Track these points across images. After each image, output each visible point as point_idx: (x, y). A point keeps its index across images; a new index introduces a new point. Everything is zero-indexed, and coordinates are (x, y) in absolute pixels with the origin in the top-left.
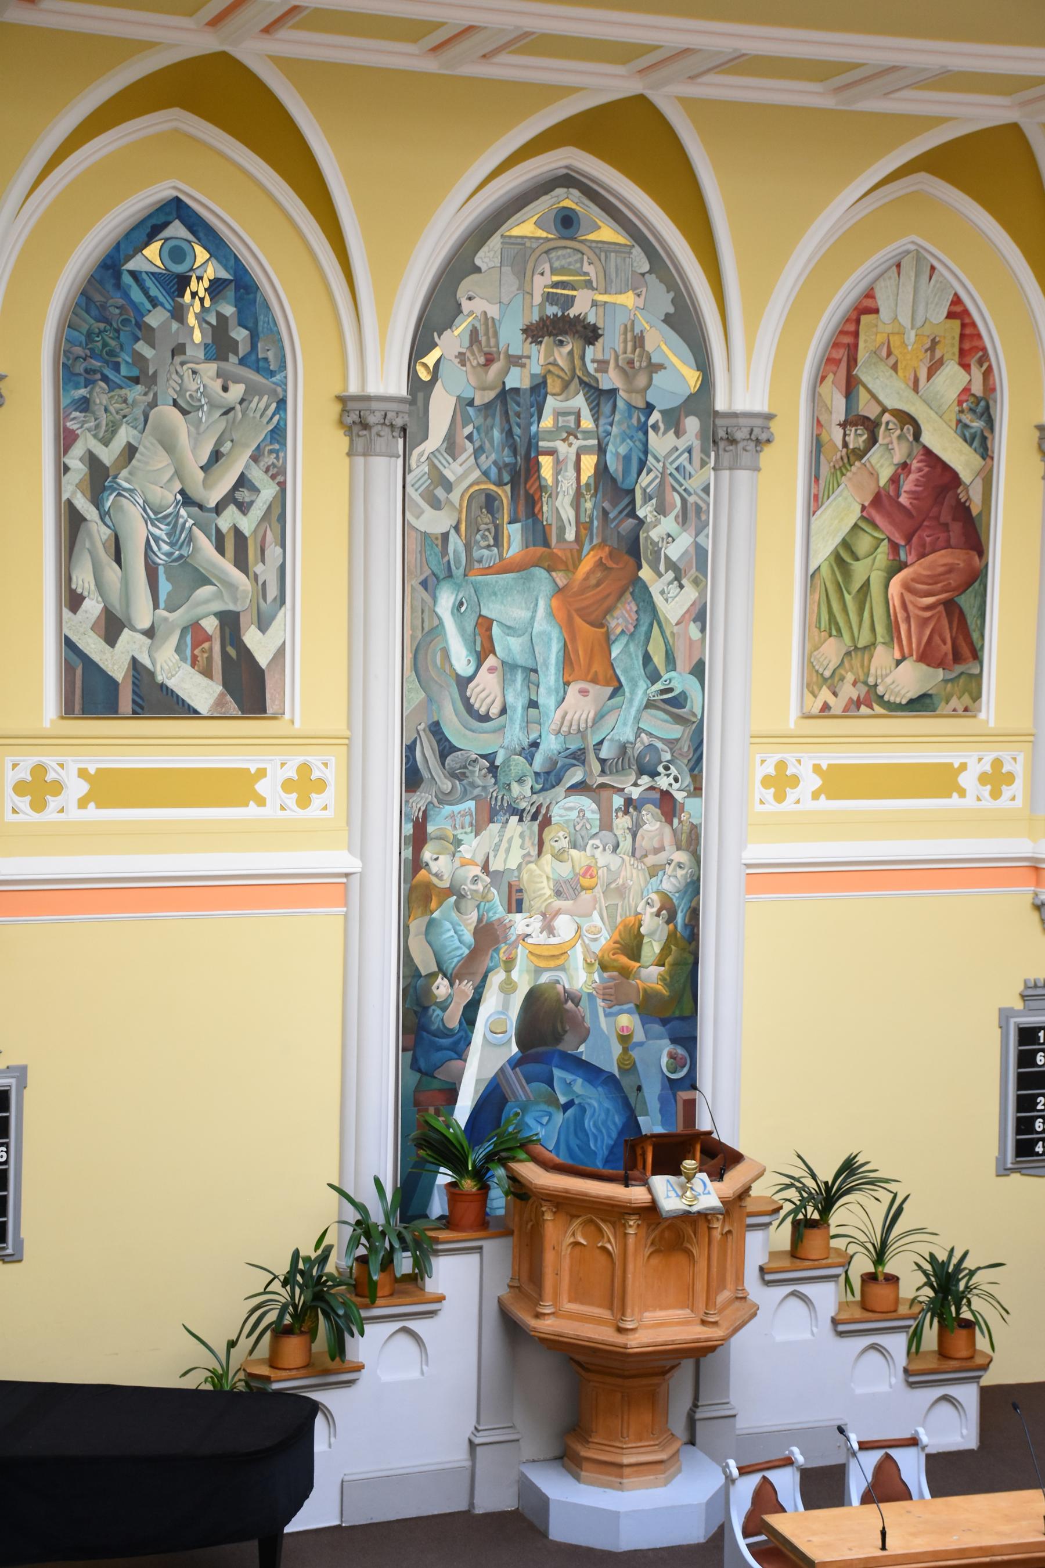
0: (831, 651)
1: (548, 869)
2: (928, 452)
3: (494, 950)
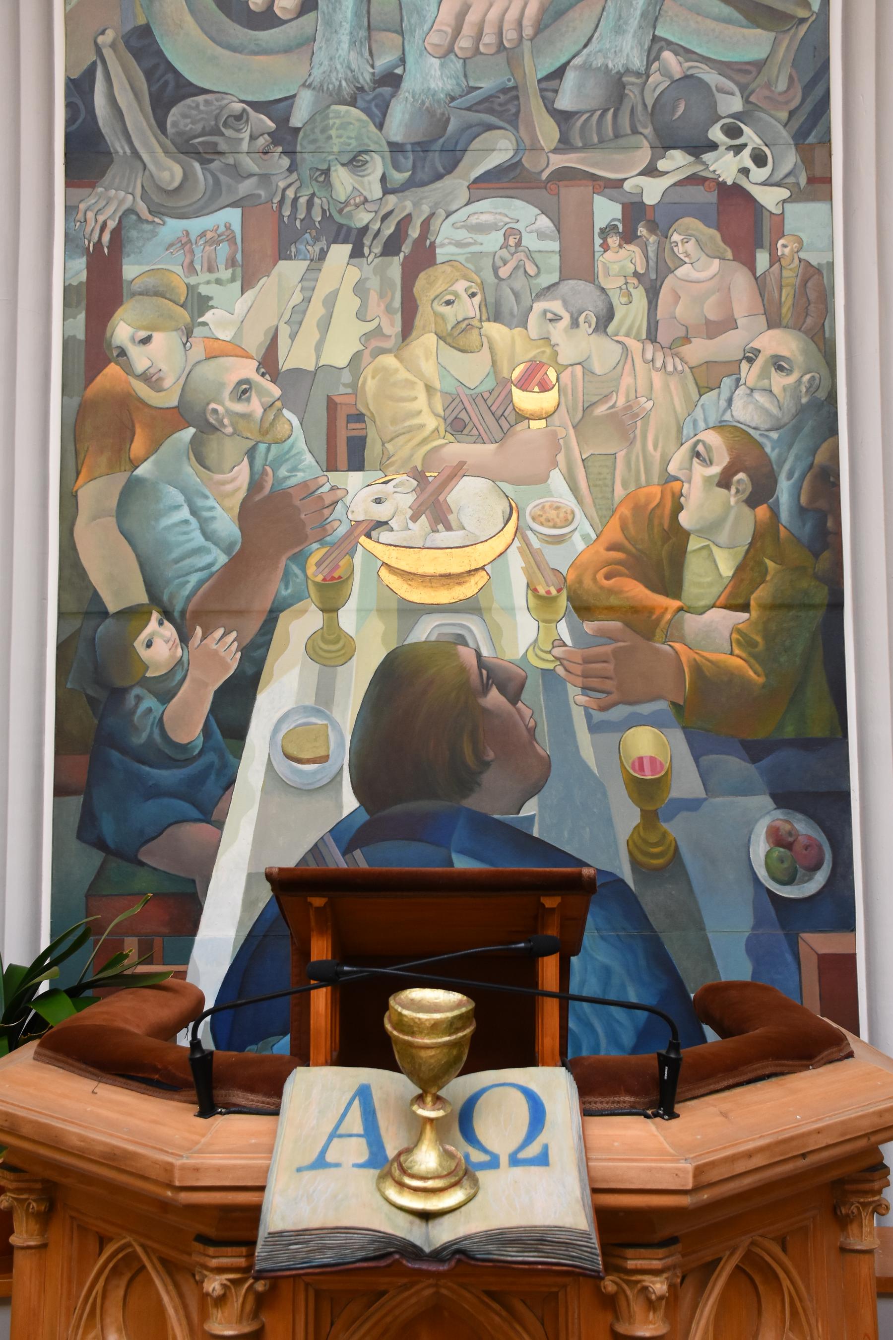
1: (429, 368)
3: (294, 558)
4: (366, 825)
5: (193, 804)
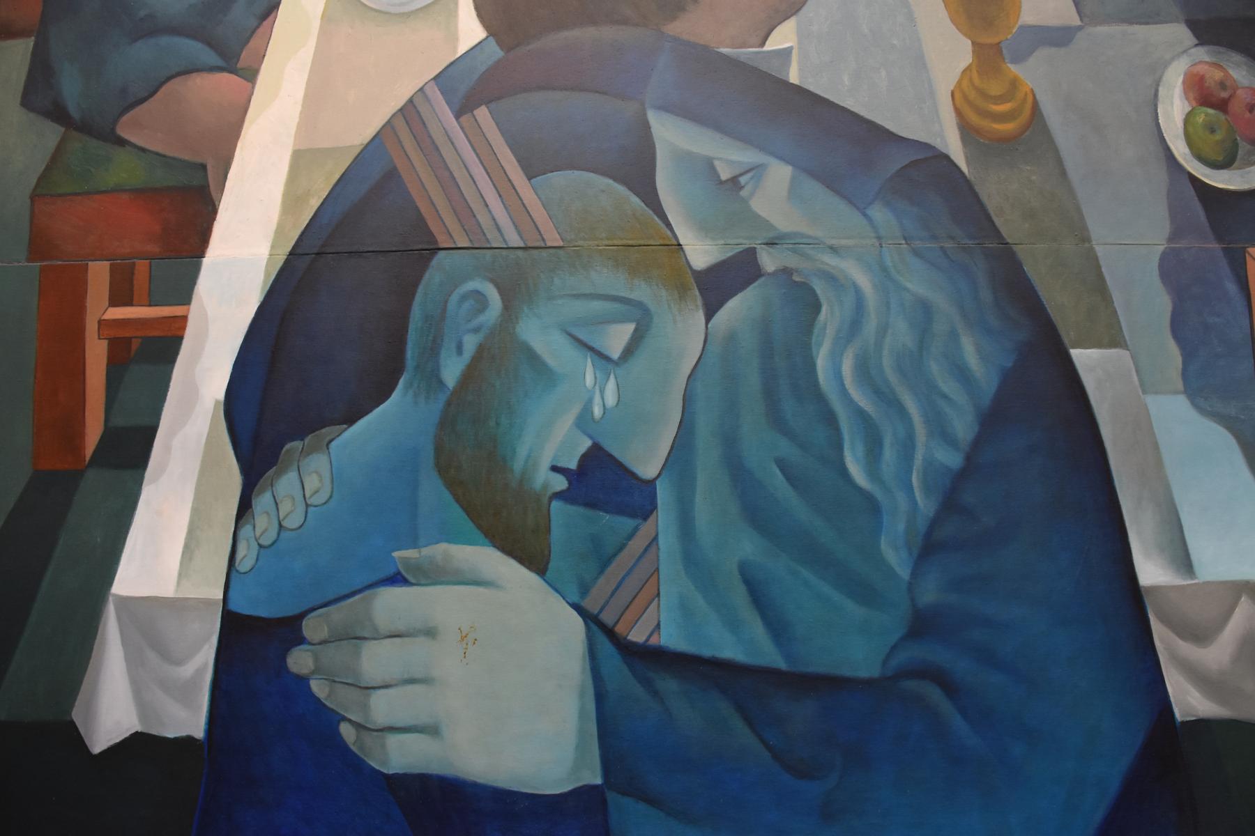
4: (497, 65)
5: (209, 45)
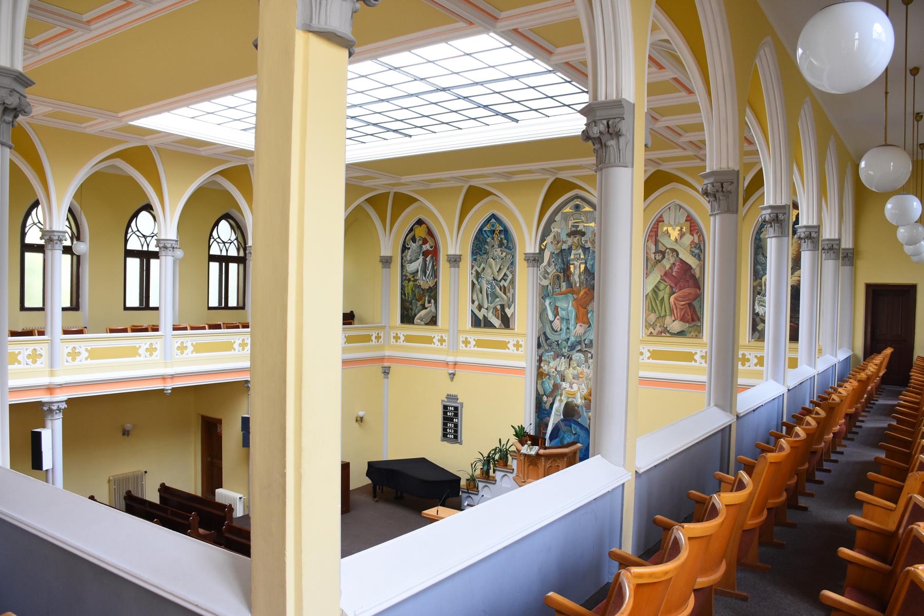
0: (653, 317)
2: (681, 260)
